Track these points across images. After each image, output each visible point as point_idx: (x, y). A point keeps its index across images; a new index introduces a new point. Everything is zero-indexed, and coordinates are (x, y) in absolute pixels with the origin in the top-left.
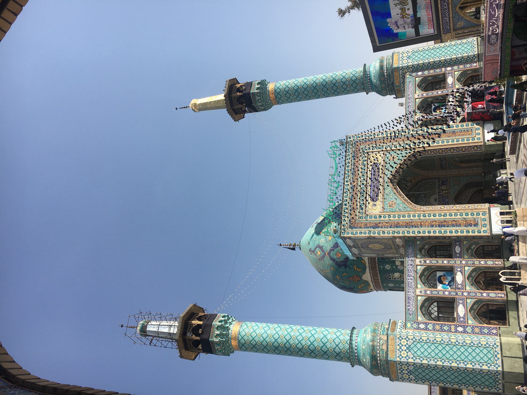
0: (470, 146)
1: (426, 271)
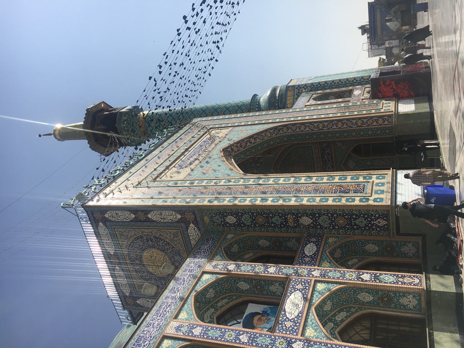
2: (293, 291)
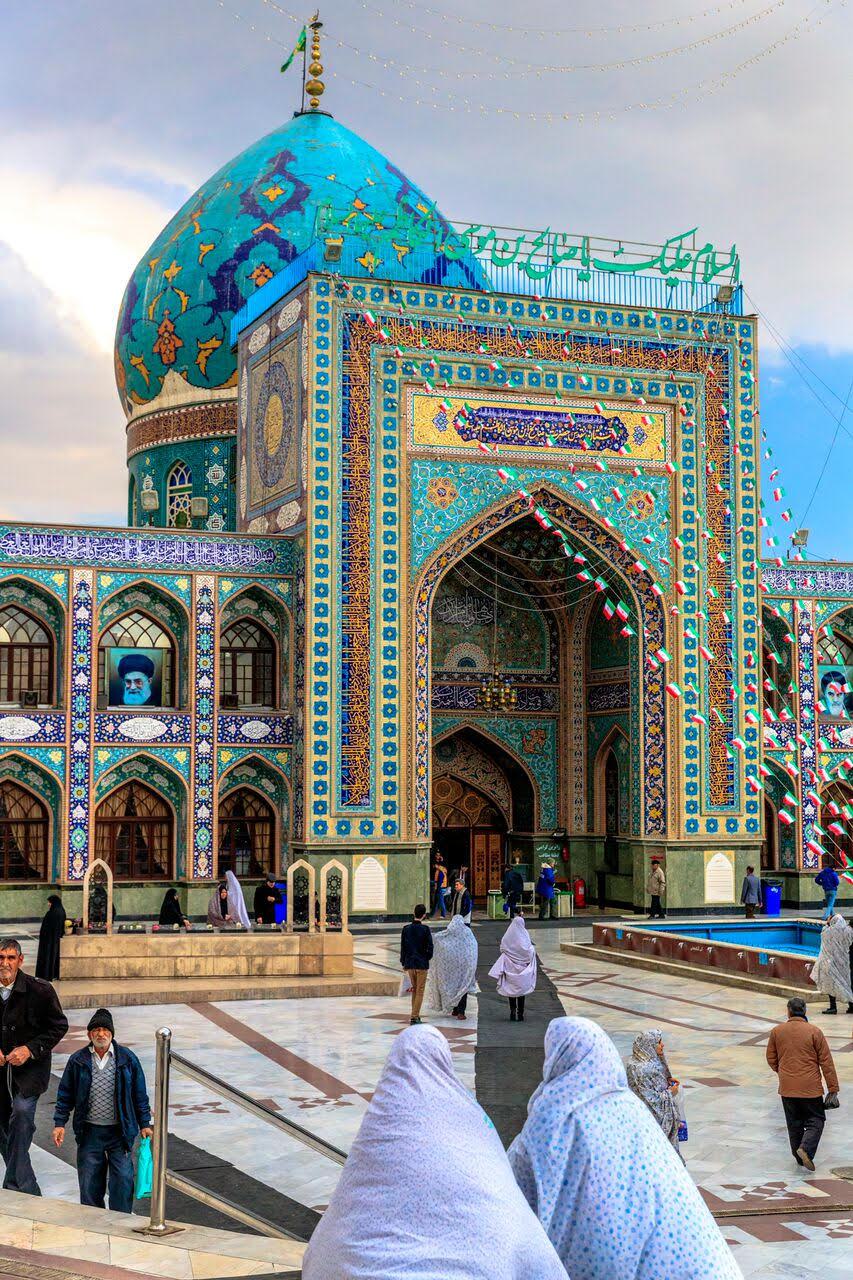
0: (664, 796)
1: (172, 610)
2: (167, 722)
